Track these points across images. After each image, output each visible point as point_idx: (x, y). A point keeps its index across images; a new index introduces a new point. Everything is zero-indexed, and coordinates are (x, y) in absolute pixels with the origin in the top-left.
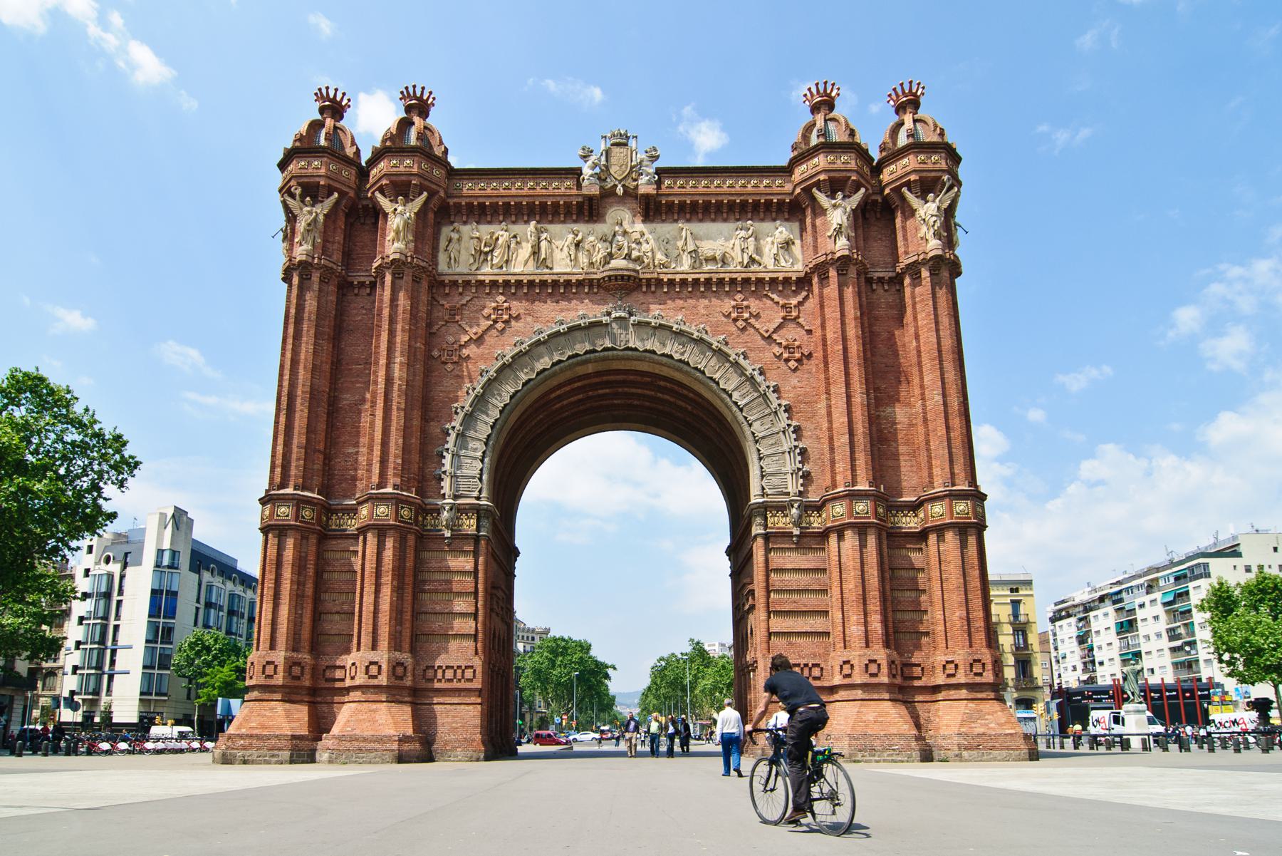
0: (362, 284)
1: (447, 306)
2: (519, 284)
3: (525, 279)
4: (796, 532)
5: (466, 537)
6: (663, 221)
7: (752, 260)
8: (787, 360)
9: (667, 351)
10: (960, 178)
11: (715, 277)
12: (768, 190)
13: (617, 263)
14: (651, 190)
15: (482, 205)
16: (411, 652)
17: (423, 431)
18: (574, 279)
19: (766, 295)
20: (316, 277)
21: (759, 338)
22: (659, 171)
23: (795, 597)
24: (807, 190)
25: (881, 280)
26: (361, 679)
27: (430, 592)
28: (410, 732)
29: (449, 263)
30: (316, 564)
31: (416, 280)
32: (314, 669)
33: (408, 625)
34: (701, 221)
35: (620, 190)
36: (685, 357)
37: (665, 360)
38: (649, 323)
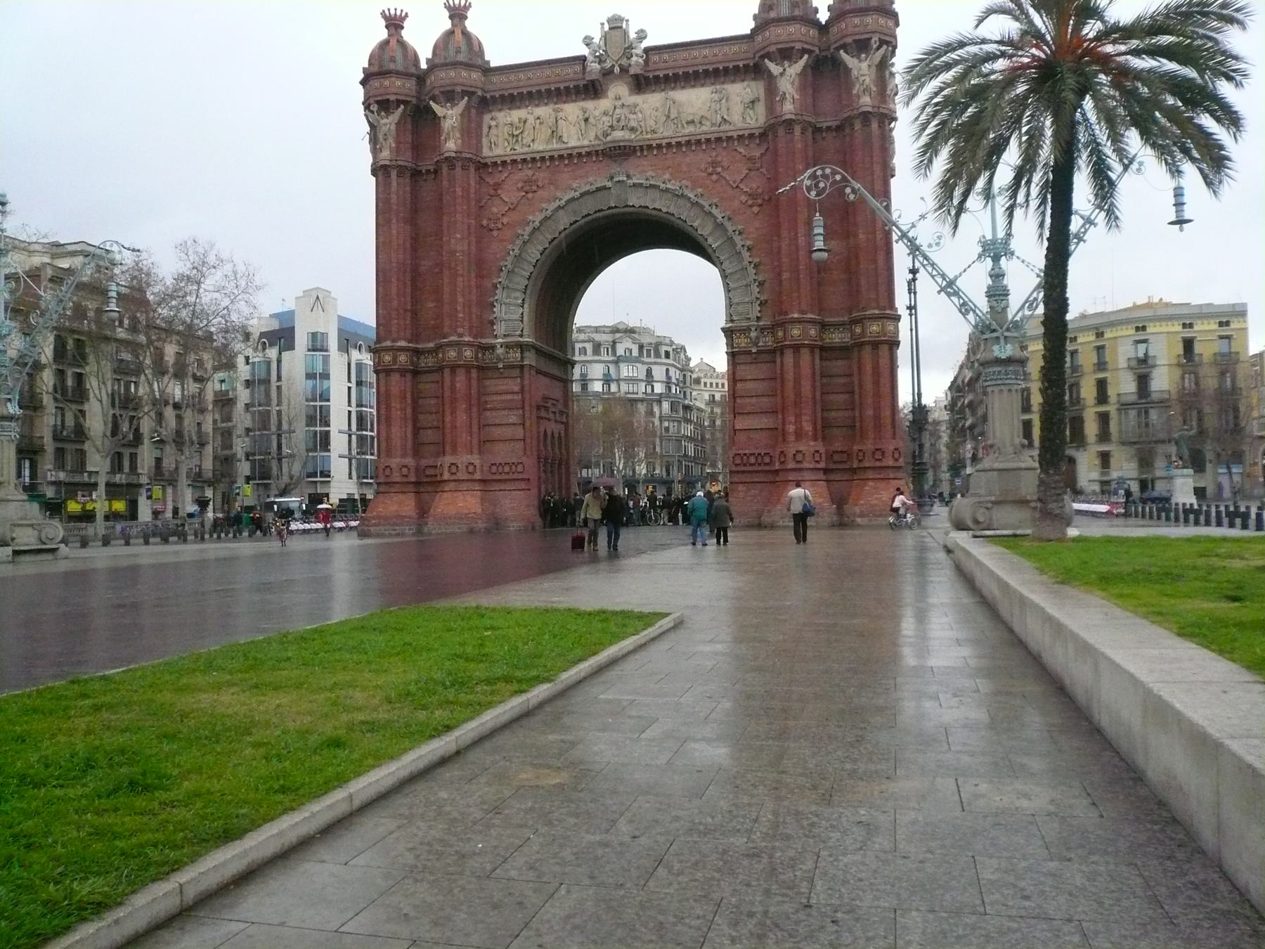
0: (428, 171)
1: (491, 182)
2: (543, 159)
3: (547, 155)
4: (754, 350)
5: (513, 367)
8: (751, 206)
13: (618, 134)
15: (511, 95)
16: (480, 453)
17: (478, 287)
18: (583, 151)
20: (394, 174)
21: (729, 188)
22: (647, 50)
23: (754, 400)
24: (763, 57)
25: (829, 128)
26: (446, 476)
27: (491, 409)
28: (480, 511)
29: (490, 148)
30: (413, 394)
31: (464, 168)
32: (417, 469)
33: (475, 436)
35: (617, 70)
36: (671, 210)
38: (641, 185)
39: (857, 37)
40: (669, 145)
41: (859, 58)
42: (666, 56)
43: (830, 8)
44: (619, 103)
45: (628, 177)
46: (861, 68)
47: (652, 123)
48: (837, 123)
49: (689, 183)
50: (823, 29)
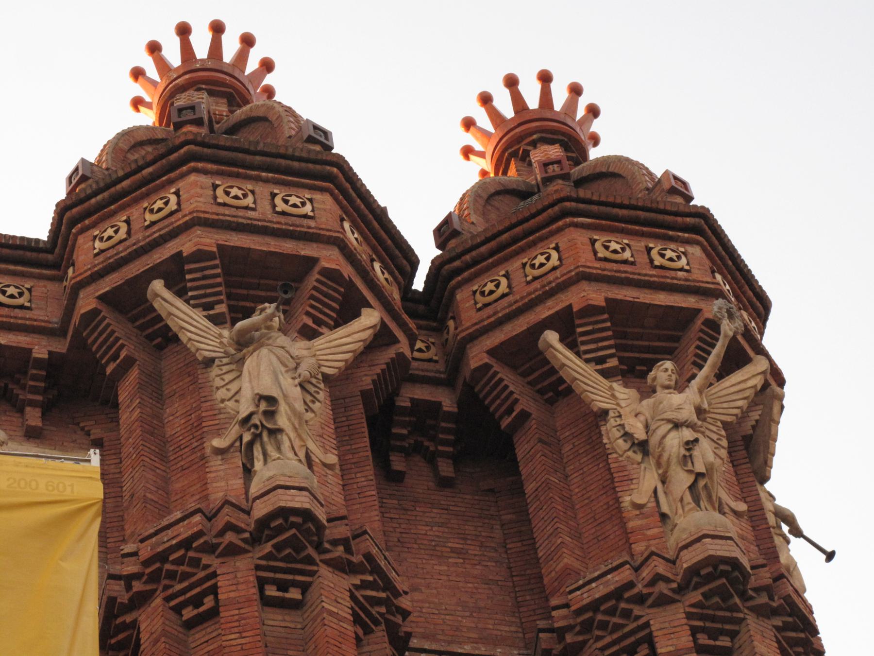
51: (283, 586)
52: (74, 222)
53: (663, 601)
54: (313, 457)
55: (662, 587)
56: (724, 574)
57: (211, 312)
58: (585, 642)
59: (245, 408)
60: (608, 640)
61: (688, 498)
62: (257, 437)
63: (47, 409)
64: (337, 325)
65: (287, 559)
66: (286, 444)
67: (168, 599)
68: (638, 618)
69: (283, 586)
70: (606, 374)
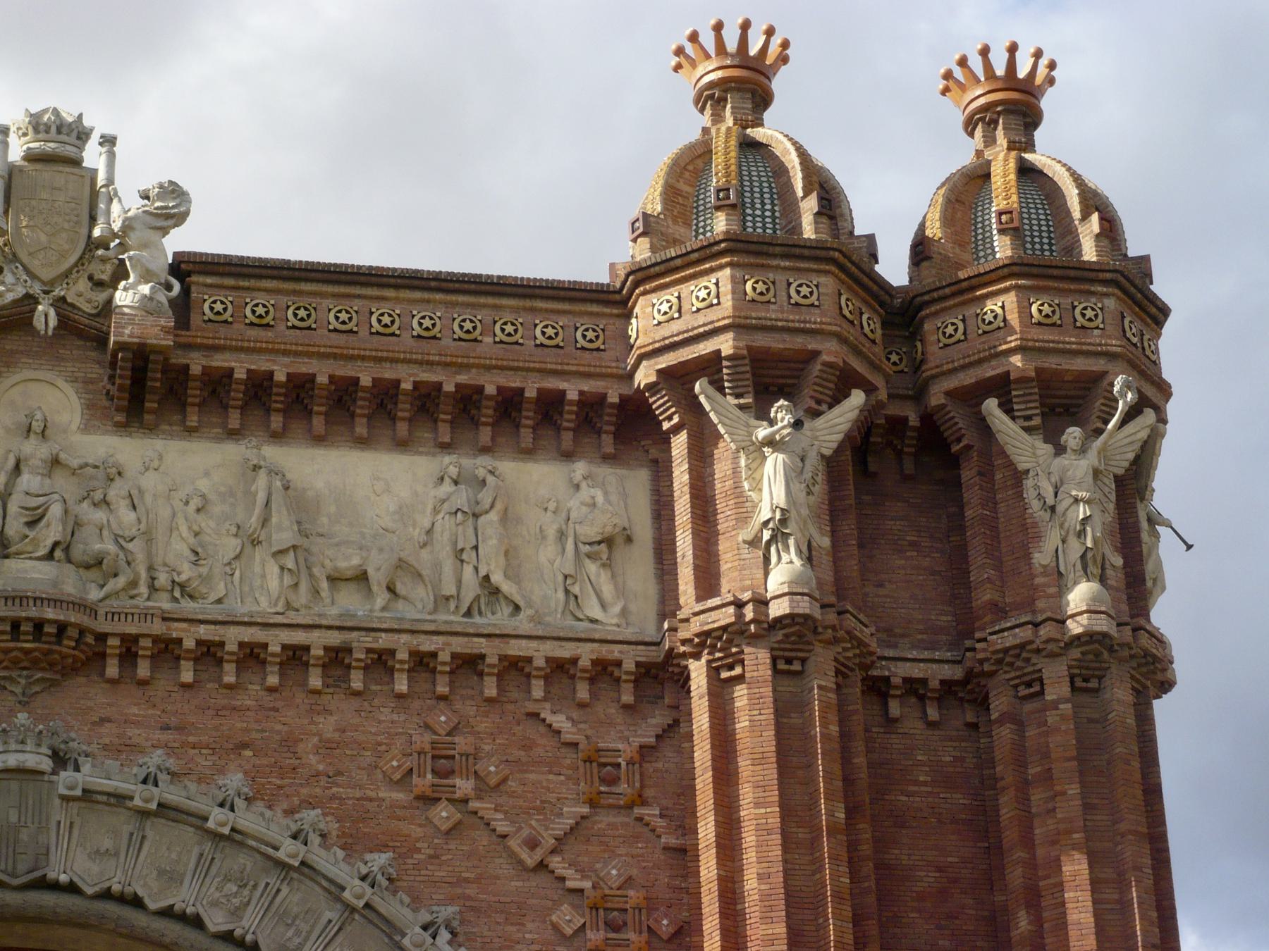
6: (191, 431)
7: (495, 592)
9: (184, 897)
10: (1167, 375)
11: (361, 643)
12: (551, 360)
14: (157, 332)
19: (535, 716)
21: (502, 867)
25: (914, 688)
34: (319, 440)
35: (45, 316)
37: (172, 930)
38: (120, 799)
39: (1052, 362)
40: (252, 655)
41: (1053, 438)
42: (258, 302)
43: (921, 250)
44: (36, 450)
45: (60, 760)
46: (1061, 480)
47: (176, 551)
48: (956, 673)
49: (333, 827)
50: (903, 315)
51: (789, 661)
52: (636, 284)
53: (1052, 655)
54: (814, 544)
55: (1050, 646)
56: (1096, 641)
57: (742, 401)
58: (997, 671)
59: (765, 514)
60: (1013, 674)
61: (1079, 566)
62: (773, 539)
63: (617, 436)
64: (831, 407)
65: (793, 643)
66: (792, 549)
67: (709, 662)
68: (1034, 664)
69: (789, 661)
70: (1027, 430)
